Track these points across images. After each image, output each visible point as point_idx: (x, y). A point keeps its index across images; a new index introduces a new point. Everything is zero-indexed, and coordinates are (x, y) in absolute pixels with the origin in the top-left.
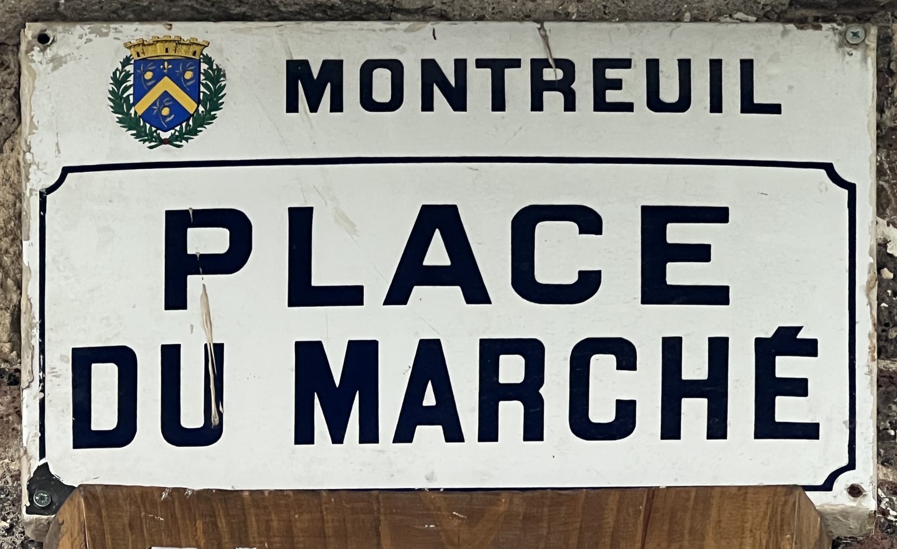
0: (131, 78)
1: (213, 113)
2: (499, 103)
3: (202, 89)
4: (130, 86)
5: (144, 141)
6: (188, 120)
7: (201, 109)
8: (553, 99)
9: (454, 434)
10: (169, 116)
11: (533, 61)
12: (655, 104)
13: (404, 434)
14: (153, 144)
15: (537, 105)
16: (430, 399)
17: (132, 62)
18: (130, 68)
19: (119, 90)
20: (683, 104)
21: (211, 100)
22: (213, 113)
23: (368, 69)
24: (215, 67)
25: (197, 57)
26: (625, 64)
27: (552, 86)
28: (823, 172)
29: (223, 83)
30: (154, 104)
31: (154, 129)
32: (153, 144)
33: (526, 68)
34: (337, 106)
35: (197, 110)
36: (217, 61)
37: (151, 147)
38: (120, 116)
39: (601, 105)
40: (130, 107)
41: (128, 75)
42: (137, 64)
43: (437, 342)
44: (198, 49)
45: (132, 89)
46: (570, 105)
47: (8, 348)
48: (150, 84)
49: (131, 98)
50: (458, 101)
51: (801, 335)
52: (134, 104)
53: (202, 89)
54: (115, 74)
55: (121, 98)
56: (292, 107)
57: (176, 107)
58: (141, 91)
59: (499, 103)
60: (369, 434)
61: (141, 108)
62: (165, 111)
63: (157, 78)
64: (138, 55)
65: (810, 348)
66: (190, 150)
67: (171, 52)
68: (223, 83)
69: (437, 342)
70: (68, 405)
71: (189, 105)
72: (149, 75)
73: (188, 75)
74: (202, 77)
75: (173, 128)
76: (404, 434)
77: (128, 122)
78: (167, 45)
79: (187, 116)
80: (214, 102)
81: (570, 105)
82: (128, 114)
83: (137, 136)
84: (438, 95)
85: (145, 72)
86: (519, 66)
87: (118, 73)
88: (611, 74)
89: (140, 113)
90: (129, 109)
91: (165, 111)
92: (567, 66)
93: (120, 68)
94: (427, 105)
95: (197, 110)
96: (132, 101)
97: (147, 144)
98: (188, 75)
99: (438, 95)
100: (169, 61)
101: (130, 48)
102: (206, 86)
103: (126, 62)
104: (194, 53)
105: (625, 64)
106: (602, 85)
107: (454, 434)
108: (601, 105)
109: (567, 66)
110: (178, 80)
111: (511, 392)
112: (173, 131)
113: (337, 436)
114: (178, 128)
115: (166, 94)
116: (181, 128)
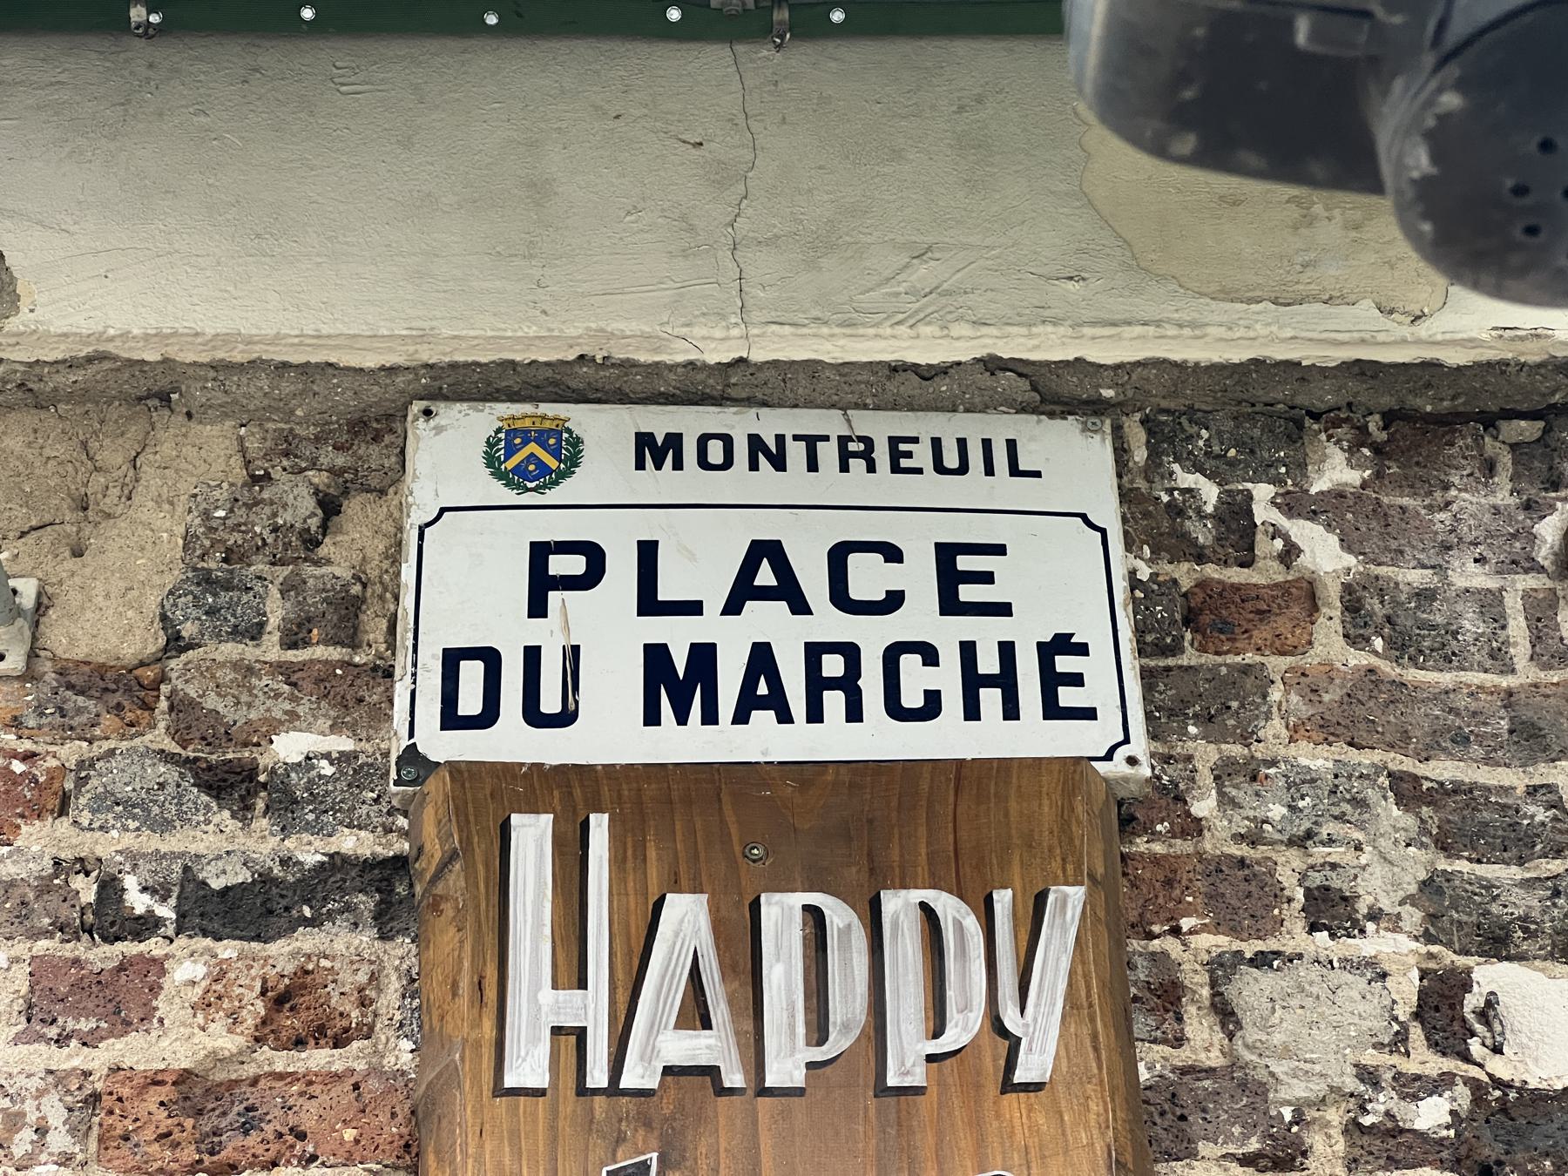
2: (813, 466)
7: (562, 466)
8: (857, 465)
9: (785, 717)
13: (741, 717)
15: (844, 468)
16: (763, 689)
18: (502, 436)
21: (571, 460)
23: (703, 441)
26: (915, 440)
27: (856, 455)
30: (522, 461)
33: (834, 443)
36: (577, 431)
39: (896, 469)
41: (500, 440)
46: (871, 468)
50: (779, 463)
56: (640, 465)
57: (541, 464)
59: (813, 466)
60: (710, 717)
61: (511, 464)
62: (532, 467)
63: (525, 443)
65: (1082, 649)
66: (552, 496)
67: (537, 425)
71: (553, 463)
73: (552, 441)
76: (741, 717)
77: (499, 475)
80: (573, 461)
82: (499, 468)
83: (506, 485)
85: (515, 438)
88: (903, 447)
91: (532, 467)
94: (754, 466)
102: (567, 450)
105: (915, 440)
106: (896, 456)
107: (785, 717)
108: (896, 469)
110: (544, 446)
111: (833, 684)
115: (532, 454)
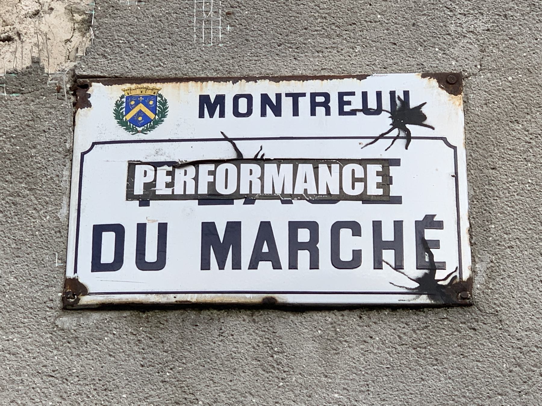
0: (124, 104)
1: (162, 119)
2: (296, 113)
3: (158, 108)
4: (124, 107)
5: (130, 132)
6: (151, 122)
7: (157, 117)
8: (320, 110)
9: (277, 266)
10: (142, 120)
11: (311, 93)
12: (366, 110)
13: (253, 266)
14: (134, 133)
15: (313, 113)
16: (265, 249)
17: (125, 97)
18: (124, 100)
19: (118, 109)
20: (379, 111)
21: (161, 113)
22: (162, 119)
23: (236, 99)
24: (164, 99)
25: (155, 95)
26: (353, 94)
27: (320, 104)
28: (441, 141)
29: (167, 106)
30: (135, 115)
31: (134, 126)
32: (134, 133)
33: (308, 96)
34: (222, 114)
35: (155, 118)
36: (165, 96)
37: (132, 134)
38: (118, 120)
39: (342, 112)
40: (123, 117)
41: (123, 102)
42: (127, 98)
43: (269, 223)
44: (156, 91)
45: (124, 109)
46: (328, 113)
47: (79, 318)
48: (133, 106)
49: (124, 113)
50: (277, 111)
51: (435, 219)
52: (125, 115)
53: (158, 108)
54: (117, 102)
55: (119, 113)
56: (201, 115)
57: (145, 116)
58: (128, 110)
59: (296, 113)
60: (237, 265)
61: (129, 117)
62: (140, 119)
63: (137, 104)
64: (128, 94)
65: (439, 225)
66: (151, 135)
67: (144, 93)
68: (167, 106)
69: (269, 223)
70: (76, 184)
71: (151, 115)
72: (133, 103)
73: (151, 103)
74: (158, 103)
75: (143, 126)
76: (253, 266)
77: (122, 123)
78: (142, 90)
79: (150, 120)
80: (163, 114)
81: (328, 113)
82: (122, 119)
83: (126, 129)
84: (268, 110)
85: (131, 101)
86: (305, 96)
87: (118, 102)
88: (346, 98)
89: (128, 119)
90: (123, 117)
91: (140, 119)
92: (327, 96)
93: (119, 100)
94: (263, 114)
95: (155, 118)
96: (124, 114)
97: (131, 133)
98: (151, 103)
99: (268, 110)
100: (143, 97)
101: (124, 91)
102: (159, 107)
103: (122, 97)
104: (154, 93)
105: (353, 94)
106: (342, 103)
107: (277, 266)
108: (342, 112)
109: (327, 96)
110: (147, 105)
111: (303, 246)
112: (143, 127)
113: (221, 266)
114: (146, 126)
115: (140, 111)
116: (147, 126)
